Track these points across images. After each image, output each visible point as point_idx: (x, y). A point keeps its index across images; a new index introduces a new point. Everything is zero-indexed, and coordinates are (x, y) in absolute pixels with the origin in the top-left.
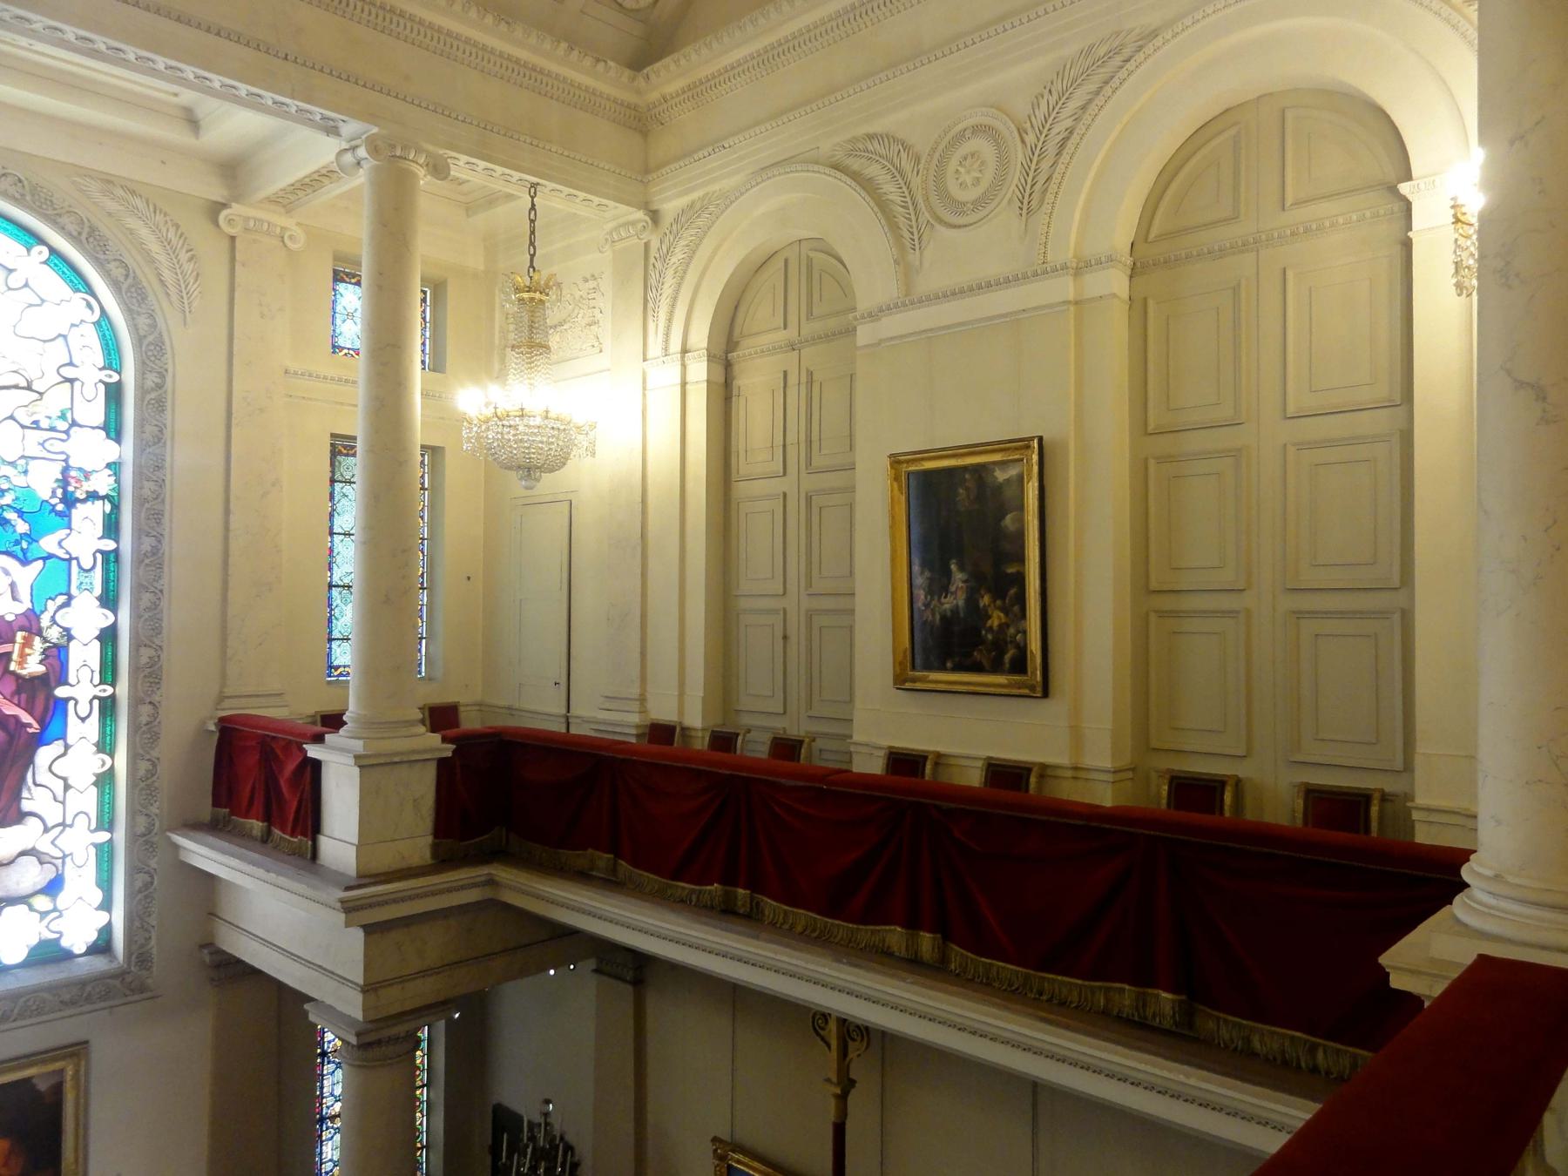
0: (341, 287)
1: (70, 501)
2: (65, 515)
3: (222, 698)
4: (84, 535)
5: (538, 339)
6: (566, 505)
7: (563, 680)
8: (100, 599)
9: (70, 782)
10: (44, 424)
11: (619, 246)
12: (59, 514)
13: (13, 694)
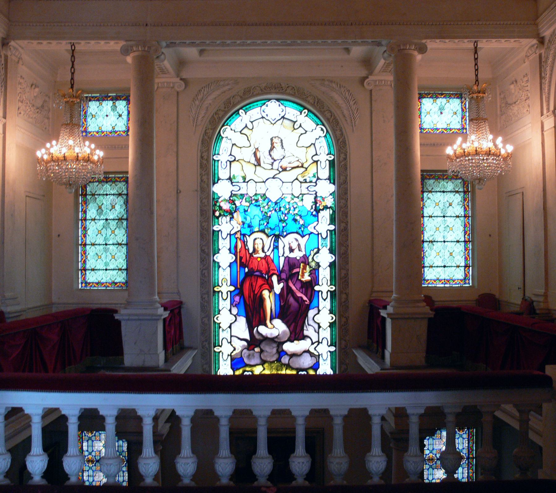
0: (424, 101)
1: (318, 211)
2: (317, 216)
3: (372, 292)
4: (324, 224)
5: (483, 114)
6: (521, 194)
7: (522, 286)
8: (329, 250)
9: (321, 325)
10: (308, 181)
11: (531, 58)
12: (314, 216)
13: (300, 289)
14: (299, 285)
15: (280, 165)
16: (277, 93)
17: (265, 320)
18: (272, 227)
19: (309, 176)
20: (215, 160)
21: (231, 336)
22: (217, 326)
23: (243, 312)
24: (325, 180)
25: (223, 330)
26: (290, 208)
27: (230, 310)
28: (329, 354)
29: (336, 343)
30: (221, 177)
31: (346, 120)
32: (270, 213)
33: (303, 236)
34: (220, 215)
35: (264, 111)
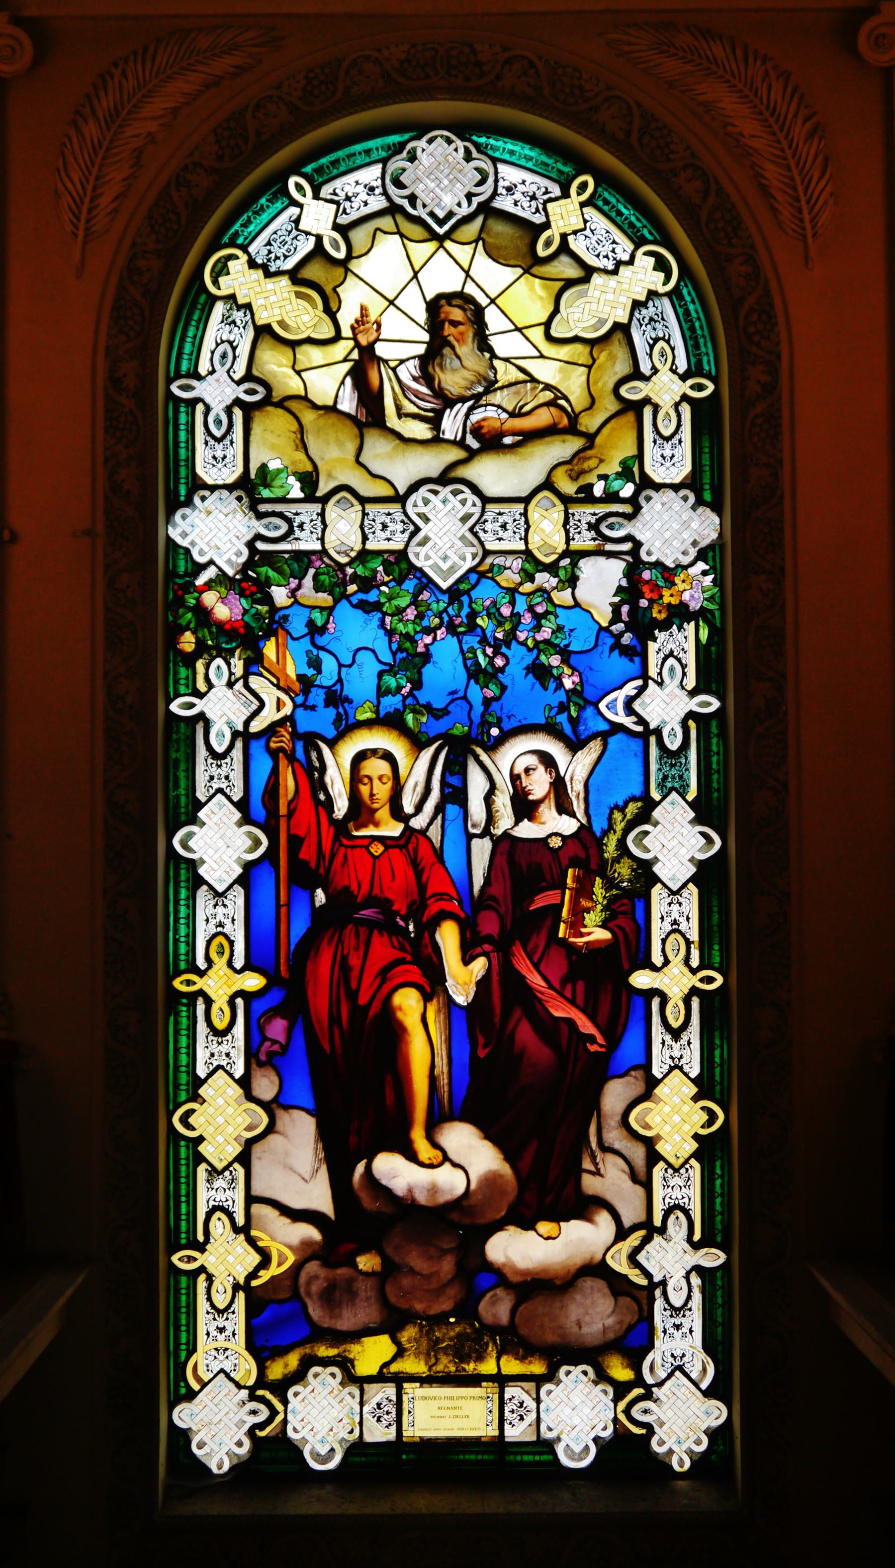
1: (644, 629)
2: (638, 653)
9: (660, 1147)
10: (598, 490)
12: (627, 652)
13: (564, 981)
14: (558, 965)
15: (475, 418)
16: (455, 93)
17: (408, 1125)
18: (438, 704)
19: (602, 470)
20: (178, 400)
21: (251, 1199)
22: (183, 1152)
23: (302, 1092)
24: (676, 488)
25: (214, 1172)
26: (516, 617)
27: (245, 1083)
28: (696, 1281)
29: (727, 1230)
30: (207, 473)
31: (774, 210)
32: (428, 640)
33: (575, 746)
34: (201, 649)
35: (399, 185)
